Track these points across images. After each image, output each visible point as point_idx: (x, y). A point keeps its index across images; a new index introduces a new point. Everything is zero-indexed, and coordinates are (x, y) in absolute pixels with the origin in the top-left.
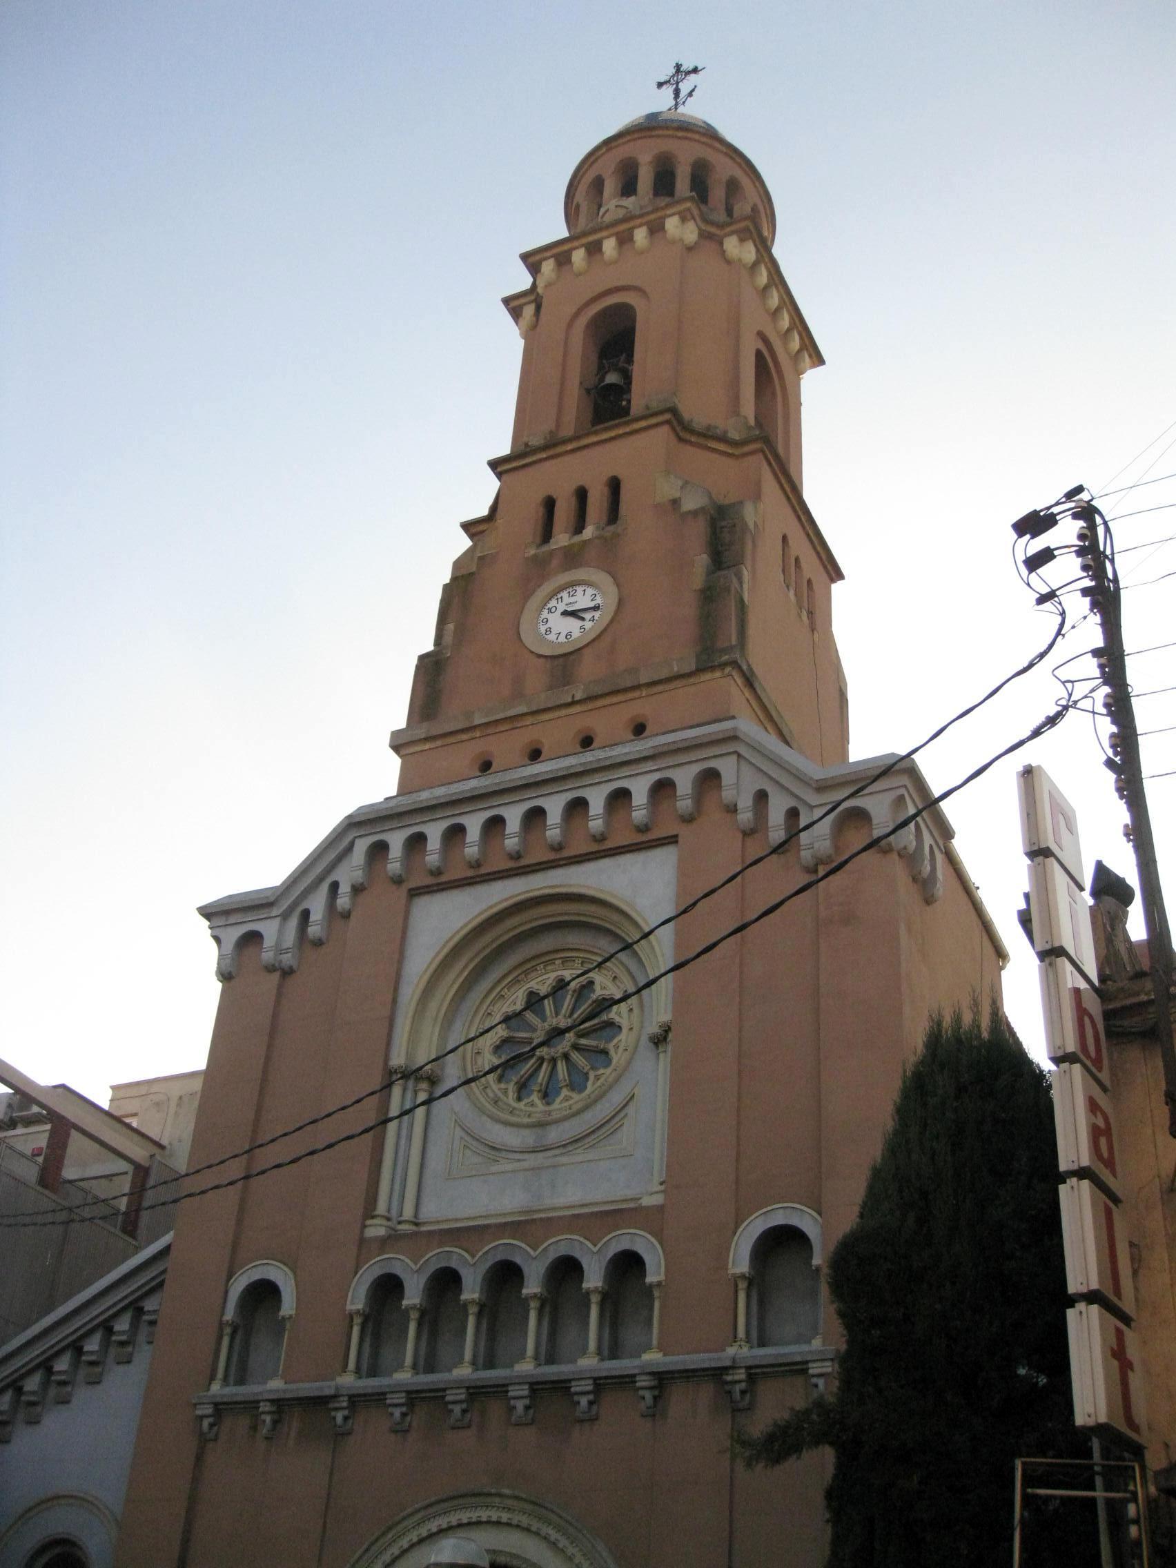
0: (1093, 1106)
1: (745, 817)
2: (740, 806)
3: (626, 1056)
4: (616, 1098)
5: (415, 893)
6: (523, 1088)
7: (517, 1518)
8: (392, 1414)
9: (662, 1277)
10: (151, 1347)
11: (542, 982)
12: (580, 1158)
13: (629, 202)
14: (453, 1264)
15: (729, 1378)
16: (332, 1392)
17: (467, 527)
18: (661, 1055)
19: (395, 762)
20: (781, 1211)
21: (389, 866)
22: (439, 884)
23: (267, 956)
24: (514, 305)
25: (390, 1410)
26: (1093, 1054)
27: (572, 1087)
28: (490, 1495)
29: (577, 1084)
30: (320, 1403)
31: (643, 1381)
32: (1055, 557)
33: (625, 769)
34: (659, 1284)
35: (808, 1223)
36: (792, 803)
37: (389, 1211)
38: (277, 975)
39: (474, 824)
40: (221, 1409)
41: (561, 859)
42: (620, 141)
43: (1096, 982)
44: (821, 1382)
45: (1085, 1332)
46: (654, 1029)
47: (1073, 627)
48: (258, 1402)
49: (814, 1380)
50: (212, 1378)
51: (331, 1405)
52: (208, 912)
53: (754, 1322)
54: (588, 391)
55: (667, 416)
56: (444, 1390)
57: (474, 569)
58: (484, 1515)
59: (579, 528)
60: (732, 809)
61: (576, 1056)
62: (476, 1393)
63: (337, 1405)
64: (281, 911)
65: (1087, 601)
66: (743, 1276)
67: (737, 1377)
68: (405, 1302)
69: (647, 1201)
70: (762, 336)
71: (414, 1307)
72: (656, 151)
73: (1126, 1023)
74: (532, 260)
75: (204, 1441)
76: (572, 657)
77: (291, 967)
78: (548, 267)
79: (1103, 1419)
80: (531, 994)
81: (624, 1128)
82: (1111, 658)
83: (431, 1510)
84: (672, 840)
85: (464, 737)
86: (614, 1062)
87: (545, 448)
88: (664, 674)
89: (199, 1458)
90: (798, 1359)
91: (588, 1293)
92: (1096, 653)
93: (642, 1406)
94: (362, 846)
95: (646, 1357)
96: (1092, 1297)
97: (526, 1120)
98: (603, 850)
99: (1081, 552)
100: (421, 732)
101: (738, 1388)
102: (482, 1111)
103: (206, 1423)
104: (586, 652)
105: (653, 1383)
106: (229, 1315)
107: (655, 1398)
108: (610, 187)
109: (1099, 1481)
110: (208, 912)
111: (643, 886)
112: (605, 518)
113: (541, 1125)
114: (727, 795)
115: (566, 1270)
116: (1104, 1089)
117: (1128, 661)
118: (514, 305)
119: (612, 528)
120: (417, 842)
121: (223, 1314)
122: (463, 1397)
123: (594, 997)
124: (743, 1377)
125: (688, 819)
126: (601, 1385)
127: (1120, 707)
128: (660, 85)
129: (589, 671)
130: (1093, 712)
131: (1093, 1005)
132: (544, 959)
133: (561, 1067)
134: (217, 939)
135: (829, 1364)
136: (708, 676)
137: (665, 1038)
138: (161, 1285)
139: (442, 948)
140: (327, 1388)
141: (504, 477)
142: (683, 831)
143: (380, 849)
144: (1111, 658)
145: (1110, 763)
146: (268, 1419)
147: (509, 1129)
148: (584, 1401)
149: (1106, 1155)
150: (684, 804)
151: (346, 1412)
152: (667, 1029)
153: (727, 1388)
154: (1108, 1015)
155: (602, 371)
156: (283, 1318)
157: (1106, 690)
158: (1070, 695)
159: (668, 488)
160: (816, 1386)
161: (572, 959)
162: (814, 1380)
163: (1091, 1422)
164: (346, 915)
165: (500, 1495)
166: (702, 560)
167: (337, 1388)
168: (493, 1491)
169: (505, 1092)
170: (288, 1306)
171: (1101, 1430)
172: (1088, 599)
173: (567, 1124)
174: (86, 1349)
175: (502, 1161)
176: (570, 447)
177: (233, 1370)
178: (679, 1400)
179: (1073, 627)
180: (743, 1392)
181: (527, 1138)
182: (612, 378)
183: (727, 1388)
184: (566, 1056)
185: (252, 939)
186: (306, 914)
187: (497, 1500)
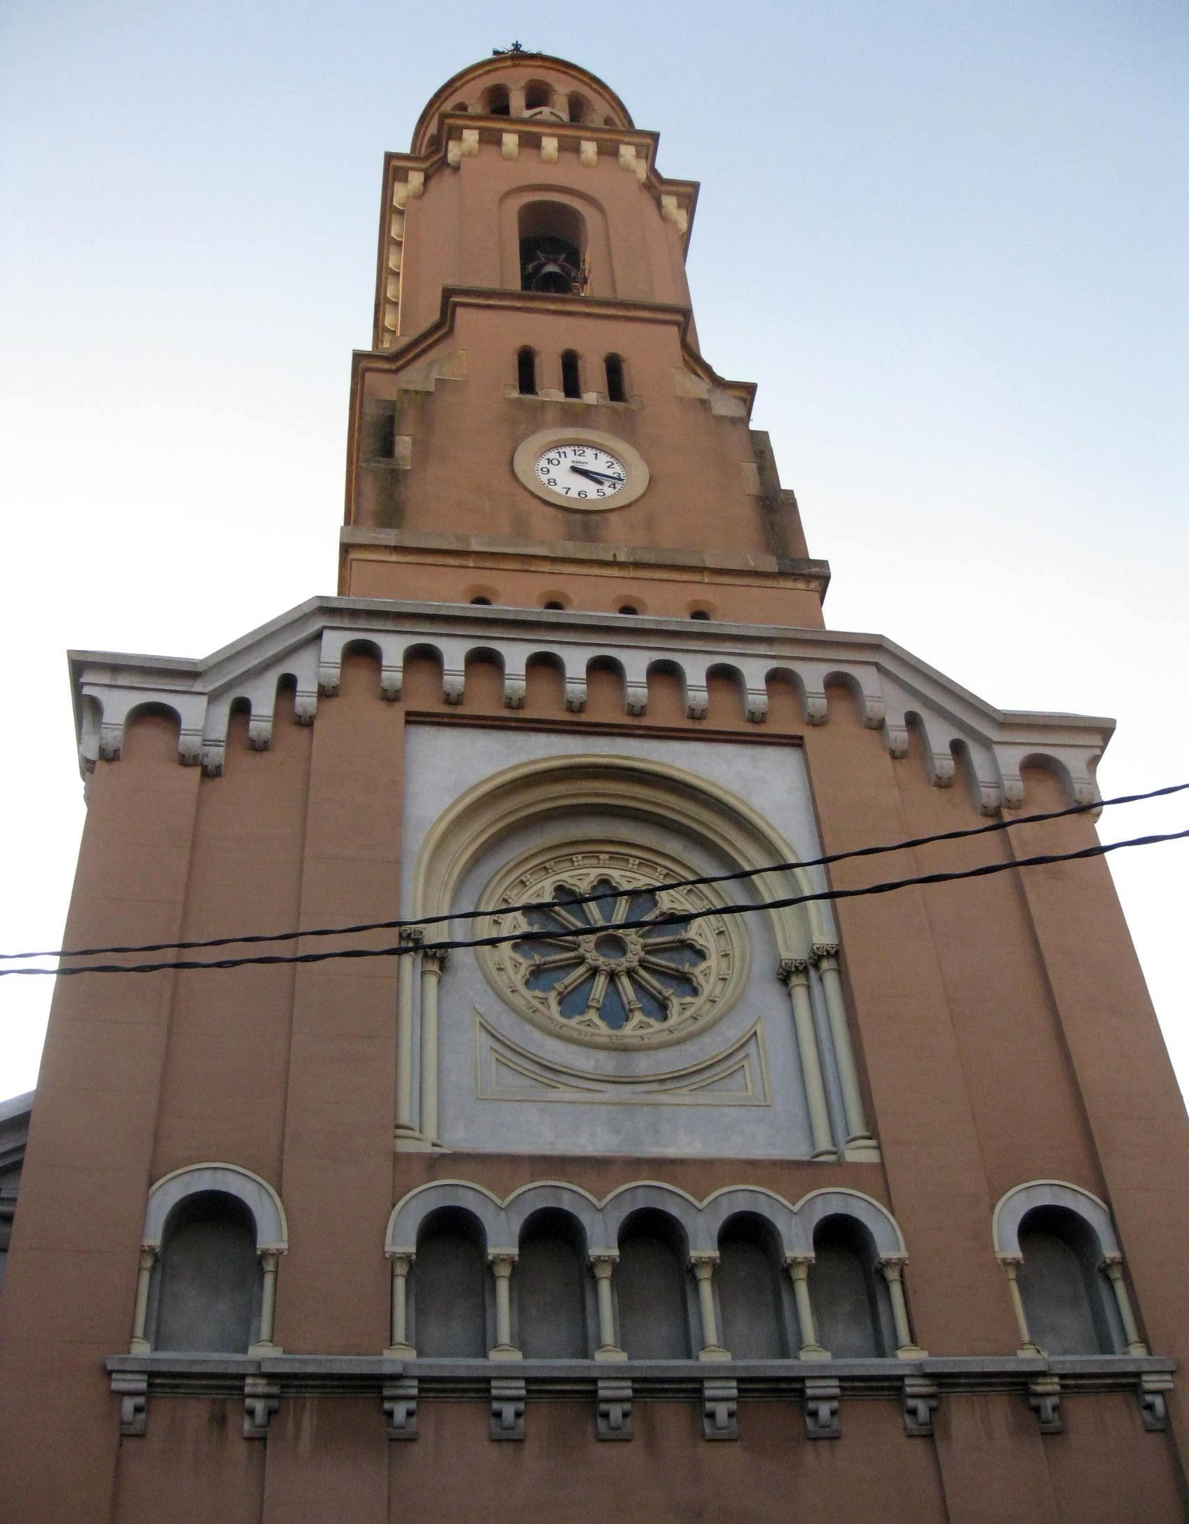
1: (898, 734)
5: (415, 719)
12: (688, 1100)
14: (567, 1203)
15: (1039, 1389)
16: (398, 1369)
22: (452, 716)
30: (373, 1386)
36: (957, 735)
38: (197, 772)
40: (162, 1382)
41: (636, 726)
48: (242, 1377)
49: (1149, 1398)
51: (386, 1392)
55: (679, 318)
60: (879, 726)
67: (1049, 1388)
72: (572, 89)
76: (594, 517)
80: (604, 882)
84: (795, 742)
94: (334, 643)
98: (695, 730)
101: (1050, 1402)
103: (129, 1404)
104: (614, 517)
106: (154, 1237)
111: (768, 787)
125: (817, 722)
129: (620, 541)
132: (589, 848)
135: (1168, 1377)
136: (789, 584)
142: (809, 734)
151: (412, 1405)
153: (1034, 1401)
162: (1149, 1398)
173: (662, 1055)
175: (562, 1088)
181: (605, 1063)
183: (1034, 1401)
184: (613, 976)
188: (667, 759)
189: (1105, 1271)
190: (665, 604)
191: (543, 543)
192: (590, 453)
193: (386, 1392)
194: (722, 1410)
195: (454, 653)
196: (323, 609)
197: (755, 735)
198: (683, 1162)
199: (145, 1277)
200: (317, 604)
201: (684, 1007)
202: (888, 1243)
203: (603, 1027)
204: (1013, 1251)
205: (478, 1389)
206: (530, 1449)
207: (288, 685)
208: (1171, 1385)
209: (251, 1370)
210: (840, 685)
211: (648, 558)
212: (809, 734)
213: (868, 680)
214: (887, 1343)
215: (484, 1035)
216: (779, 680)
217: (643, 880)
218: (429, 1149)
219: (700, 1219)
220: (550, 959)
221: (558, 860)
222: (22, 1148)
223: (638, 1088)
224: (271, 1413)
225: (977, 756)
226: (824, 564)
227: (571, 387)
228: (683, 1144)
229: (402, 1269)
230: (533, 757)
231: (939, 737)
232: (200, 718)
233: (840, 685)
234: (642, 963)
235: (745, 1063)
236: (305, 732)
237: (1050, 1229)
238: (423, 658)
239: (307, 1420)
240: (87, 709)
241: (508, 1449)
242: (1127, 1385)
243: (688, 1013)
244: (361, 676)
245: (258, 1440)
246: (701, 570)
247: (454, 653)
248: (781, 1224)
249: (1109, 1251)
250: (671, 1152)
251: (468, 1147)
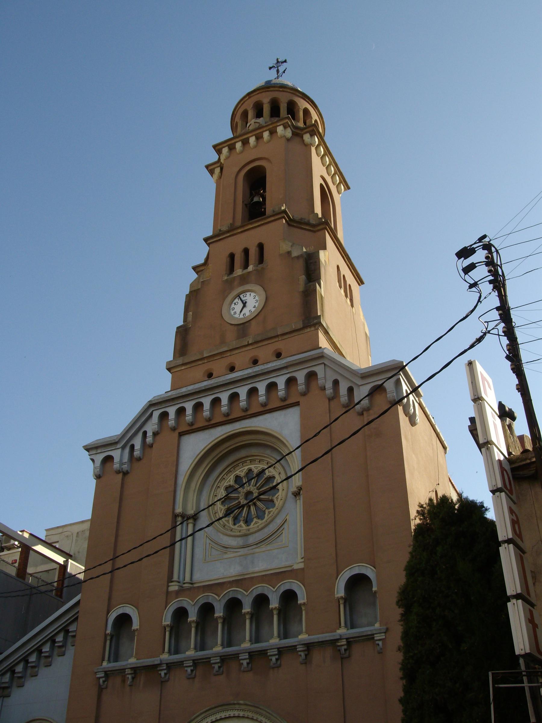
0: (511, 511)
1: (329, 391)
3: (281, 502)
4: (278, 521)
5: (181, 434)
6: (236, 520)
7: (246, 714)
9: (305, 601)
10: (74, 647)
11: (241, 471)
12: (264, 549)
13: (261, 120)
14: (210, 601)
15: (339, 644)
16: (159, 662)
17: (194, 268)
18: (298, 501)
19: (169, 375)
20: (357, 567)
21: (169, 423)
22: (193, 429)
23: (116, 466)
24: (210, 168)
25: (186, 669)
26: (509, 488)
27: (258, 517)
28: (234, 704)
29: (260, 517)
30: (154, 668)
31: (300, 648)
32: (476, 267)
33: (273, 373)
34: (304, 604)
35: (370, 572)
36: (350, 385)
37: (179, 578)
38: (121, 475)
39: (207, 402)
40: (108, 674)
41: (247, 415)
42: (254, 94)
43: (507, 456)
44: (380, 643)
45: (516, 612)
46: (295, 489)
47: (485, 298)
48: (125, 669)
49: (377, 642)
50: (103, 660)
51: (158, 669)
52: (88, 449)
53: (348, 617)
54: (246, 205)
56: (210, 658)
57: (200, 287)
58: (231, 713)
59: (246, 266)
60: (323, 389)
61: (259, 503)
62: (224, 659)
63: (161, 668)
64: (121, 445)
65: (491, 286)
66: (342, 598)
68: (189, 620)
69: (296, 567)
70: (323, 178)
71: (193, 621)
72: (270, 98)
73: (521, 473)
74: (218, 148)
75: (101, 689)
76: (247, 324)
78: (225, 151)
79: (528, 651)
81: (283, 535)
82: (504, 312)
83: (207, 713)
84: (297, 404)
85: (200, 362)
86: (277, 505)
87: (228, 232)
88: (287, 330)
90: (369, 633)
91: (272, 609)
92: (498, 309)
93: (301, 659)
95: (300, 637)
96: (518, 597)
97: (238, 534)
98: (266, 410)
99: (487, 264)
100: (180, 361)
102: (218, 531)
103: (101, 680)
106: (109, 631)
107: (306, 655)
108: (251, 114)
109: (525, 678)
110: (88, 449)
111: (286, 426)
112: (257, 263)
113: (246, 535)
114: (321, 382)
115: (261, 601)
116: (515, 503)
117: (512, 312)
118: (210, 168)
119: (261, 265)
120: (181, 411)
121: (106, 629)
122: (219, 661)
123: (265, 476)
124: (345, 643)
125: (304, 394)
126: (281, 651)
127: (510, 333)
128: (270, 68)
129: (255, 330)
130: (499, 335)
131: (507, 467)
133: (253, 508)
134: (93, 460)
135: (384, 634)
136: (309, 330)
137: (299, 493)
138: (77, 619)
139: (196, 458)
140: (156, 661)
141: (211, 245)
142: (302, 400)
143: (164, 416)
144: (504, 312)
145: (508, 357)
146: (130, 676)
147: (231, 538)
148: (274, 659)
149: (518, 533)
150: (301, 387)
151: (165, 671)
152: (300, 489)
153: (338, 648)
154: (513, 470)
155: (252, 196)
156: (134, 630)
157: (503, 325)
158: (486, 329)
159: (285, 247)
160: (378, 645)
161: (254, 460)
162: (377, 642)
163: (523, 653)
164: (151, 446)
165: (239, 704)
166: (302, 278)
167: (161, 660)
168: (235, 702)
169: (228, 521)
170: (136, 625)
171: (526, 656)
172: (492, 285)
173: (257, 534)
174: (43, 650)
175: (229, 553)
176: (239, 231)
177: (112, 655)
178: (317, 656)
179: (485, 298)
180: (345, 650)
181: (239, 541)
182: (256, 199)
183: (338, 648)
185: (108, 459)
186: (132, 447)
187: (237, 706)
193: (158, 669)
197: (285, 405)
208: (384, 637)
217: (261, 466)
220: (231, 504)
223: (250, 548)
230: (217, 437)
235: (283, 531)
246: (277, 336)
249: (374, 589)
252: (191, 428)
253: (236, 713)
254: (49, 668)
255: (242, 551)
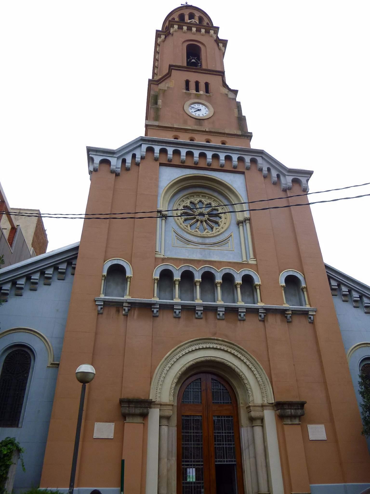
2: (263, 169)
5: (161, 164)
7: (222, 348)
8: (175, 312)
14: (191, 269)
15: (287, 313)
16: (155, 302)
22: (169, 164)
25: (175, 310)
35: (300, 276)
38: (114, 175)
40: (107, 304)
41: (209, 168)
44: (312, 317)
49: (310, 316)
51: (152, 307)
60: (261, 170)
63: (156, 307)
77: (119, 173)
84: (243, 173)
89: (97, 319)
94: (144, 147)
98: (222, 170)
101: (289, 316)
103: (100, 307)
104: (206, 121)
105: (264, 311)
106: (105, 273)
107: (265, 316)
111: (236, 182)
125: (248, 169)
132: (198, 194)
139: (171, 182)
142: (246, 172)
147: (193, 237)
153: (286, 315)
162: (310, 316)
165: (217, 340)
173: (211, 239)
183: (286, 315)
187: (216, 341)
188: (215, 175)
189: (302, 289)
190: (216, 142)
191: (189, 126)
192: (201, 105)
193: (152, 307)
194: (221, 314)
195: (170, 150)
196: (142, 139)
197: (234, 171)
198: (215, 262)
199: (103, 281)
200: (141, 138)
201: (216, 229)
202: (257, 281)
203: (199, 233)
204: (284, 284)
205: (171, 307)
206: (181, 320)
207: (134, 156)
209: (125, 301)
210: (253, 161)
211: (213, 130)
212: (246, 172)
213: (260, 160)
214: (256, 302)
215: (174, 233)
216: (241, 159)
218: (162, 257)
219: (219, 274)
221: (191, 196)
222: (77, 253)
224: (129, 310)
225: (282, 178)
226: (251, 133)
227: (197, 90)
228: (215, 258)
229: (156, 282)
231: (274, 173)
232: (115, 163)
233: (253, 161)
234: (208, 219)
236: (138, 167)
237: (292, 281)
238: (163, 151)
239: (136, 313)
240: (91, 160)
241: (177, 319)
242: (305, 313)
243: (218, 230)
244: (150, 154)
245: (126, 315)
247: (170, 150)
248: (235, 276)
249: (303, 285)
250: (213, 259)
251: (170, 256)
252: (169, 163)
253: (215, 346)
254: (34, 292)
255: (201, 246)
